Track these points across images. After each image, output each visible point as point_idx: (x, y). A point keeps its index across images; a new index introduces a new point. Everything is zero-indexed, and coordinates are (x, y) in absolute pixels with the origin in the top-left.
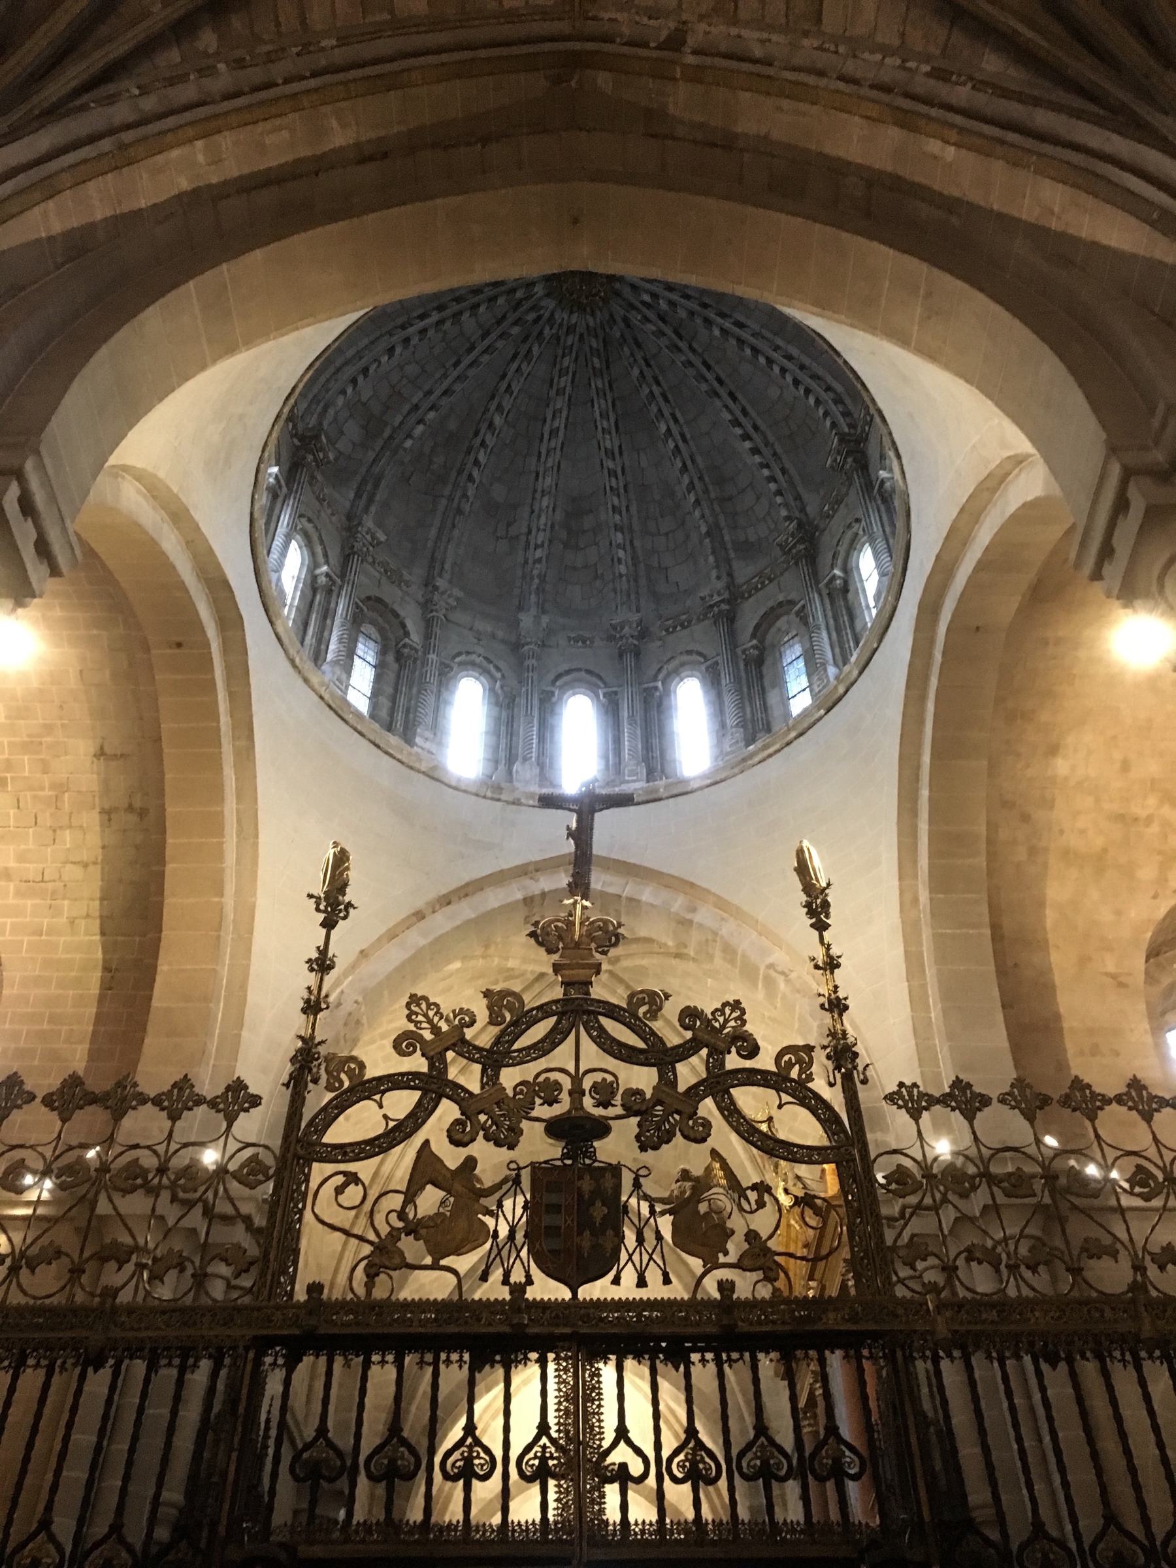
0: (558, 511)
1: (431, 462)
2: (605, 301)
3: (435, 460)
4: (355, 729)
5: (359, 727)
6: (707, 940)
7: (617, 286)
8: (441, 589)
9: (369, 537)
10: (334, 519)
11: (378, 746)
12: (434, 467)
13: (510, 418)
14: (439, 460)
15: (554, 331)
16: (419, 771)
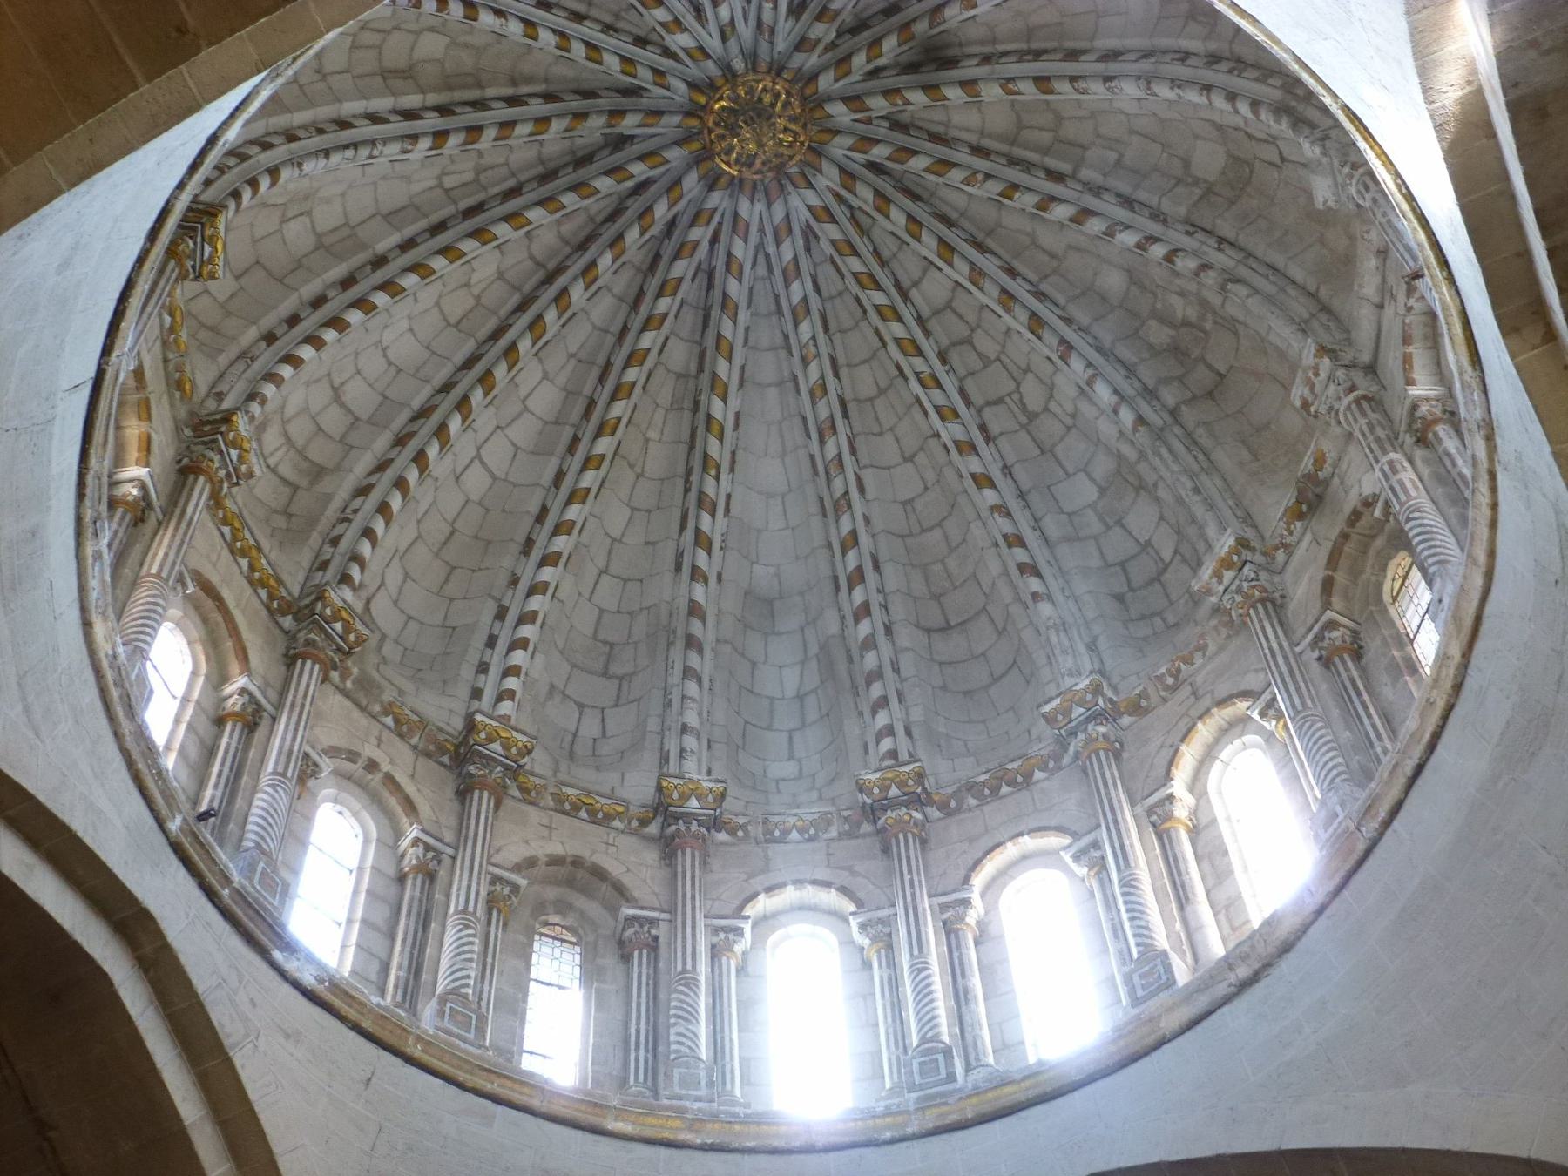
0: (1186, 44)
1: (1186, 323)
2: (777, 69)
3: (1179, 315)
4: (1387, 823)
5: (1383, 814)
6: (1548, 52)
7: (738, 65)
8: (1306, 391)
9: (1228, 575)
10: (1212, 648)
11: (1419, 769)
12: (1192, 313)
13: (1065, 167)
14: (1181, 309)
15: (882, 130)
16: (1465, 665)
